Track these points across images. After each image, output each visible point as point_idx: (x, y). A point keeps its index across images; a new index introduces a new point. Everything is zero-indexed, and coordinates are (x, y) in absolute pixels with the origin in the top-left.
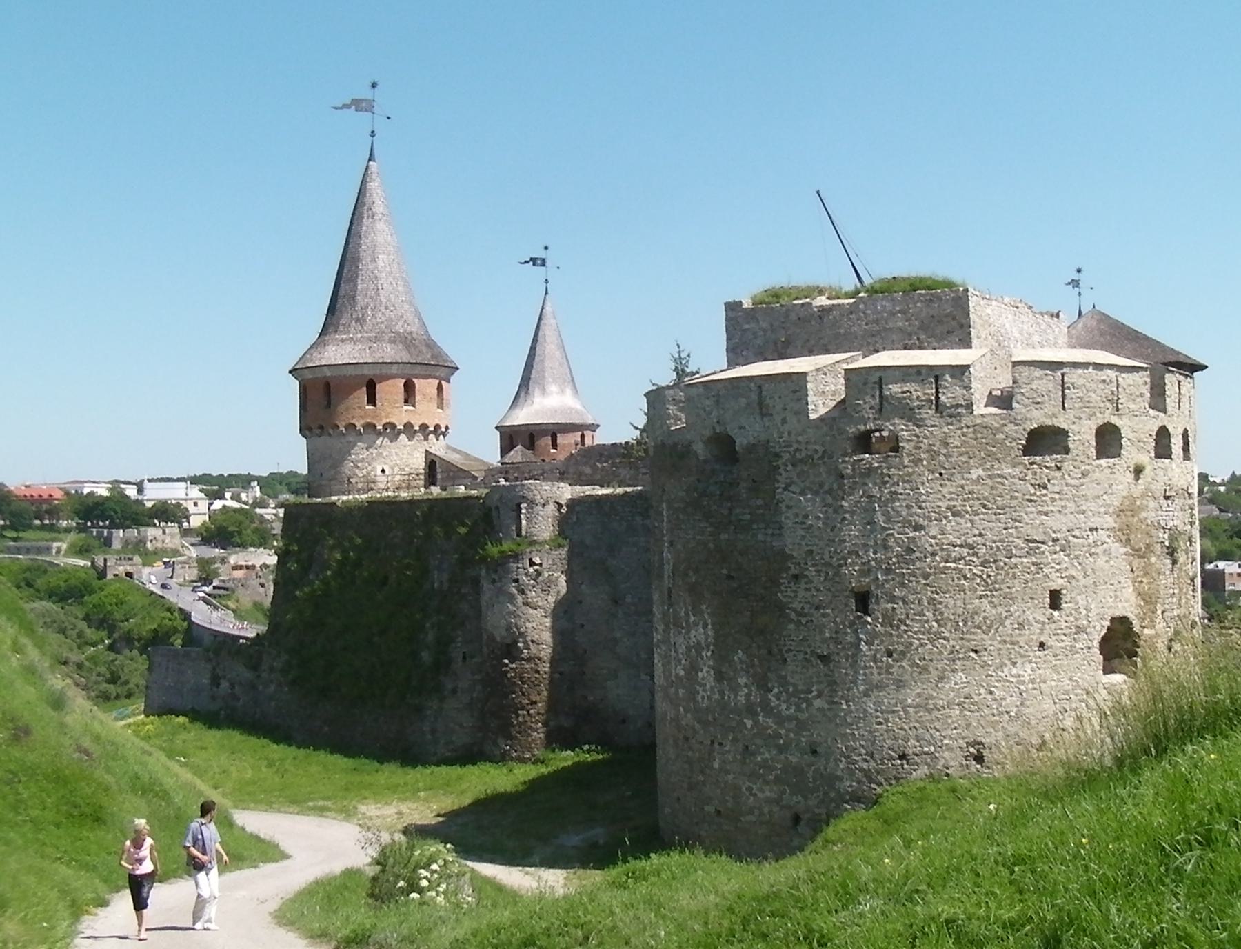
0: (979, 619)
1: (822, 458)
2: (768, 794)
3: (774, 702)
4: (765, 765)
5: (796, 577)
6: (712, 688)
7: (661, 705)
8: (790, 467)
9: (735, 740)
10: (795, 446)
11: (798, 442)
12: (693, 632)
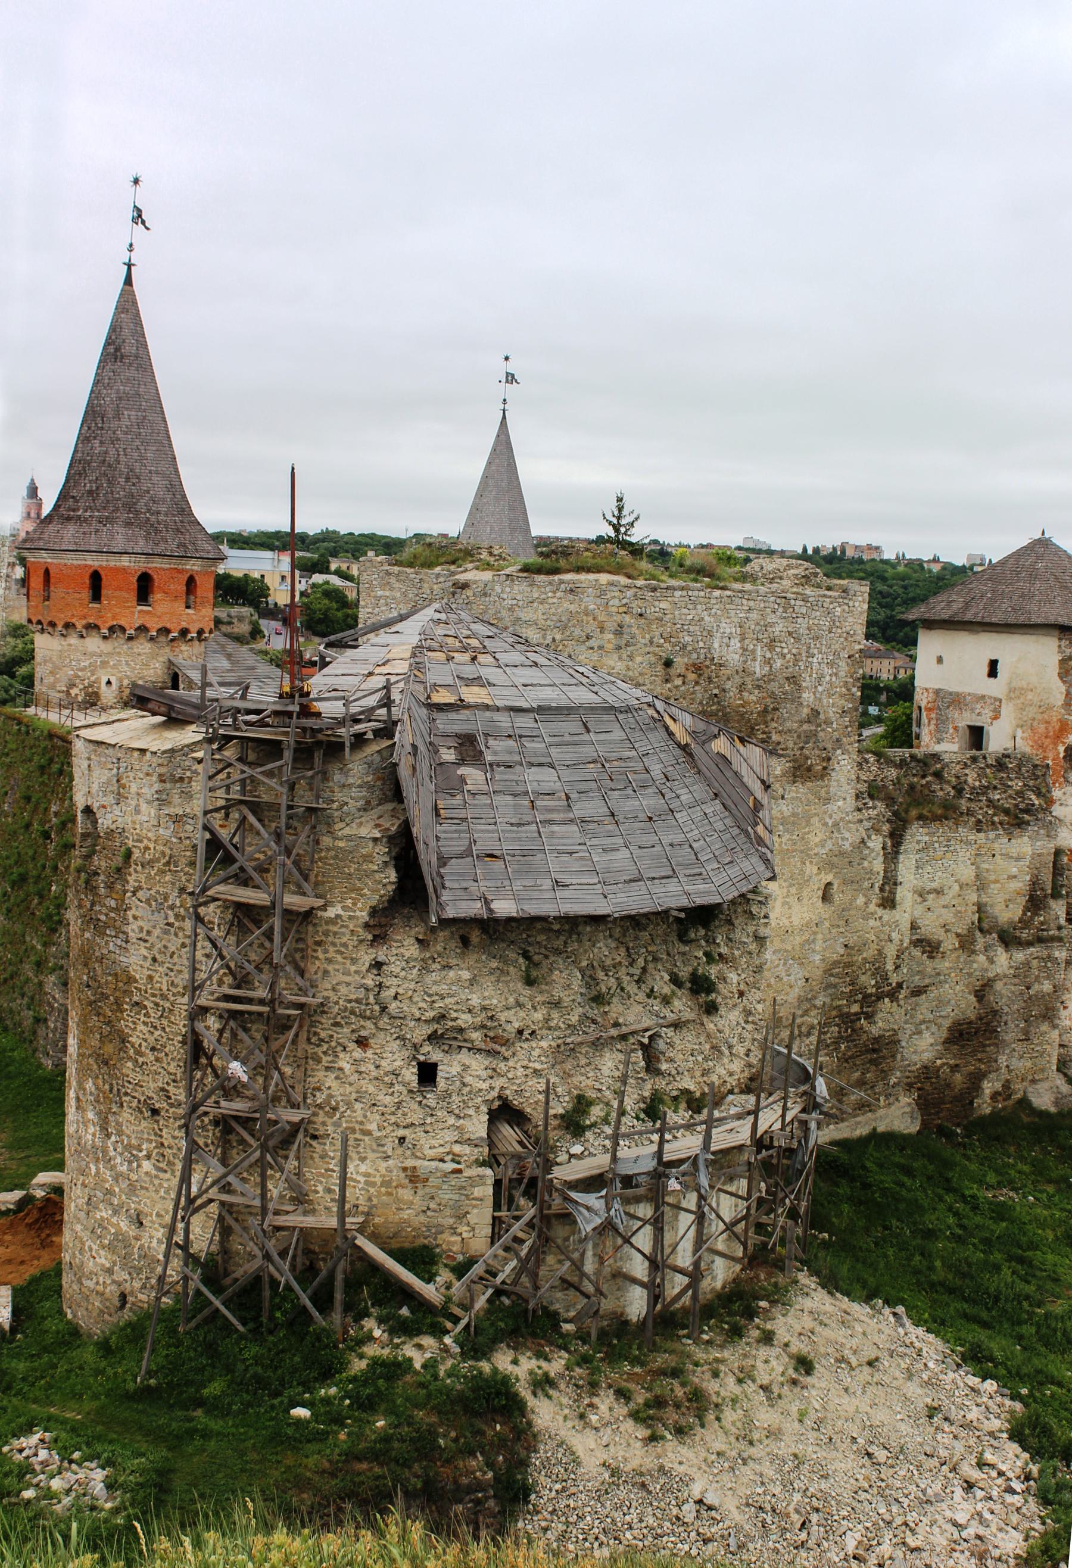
0: (320, 1098)
1: (168, 863)
2: (103, 1261)
8: (139, 868)
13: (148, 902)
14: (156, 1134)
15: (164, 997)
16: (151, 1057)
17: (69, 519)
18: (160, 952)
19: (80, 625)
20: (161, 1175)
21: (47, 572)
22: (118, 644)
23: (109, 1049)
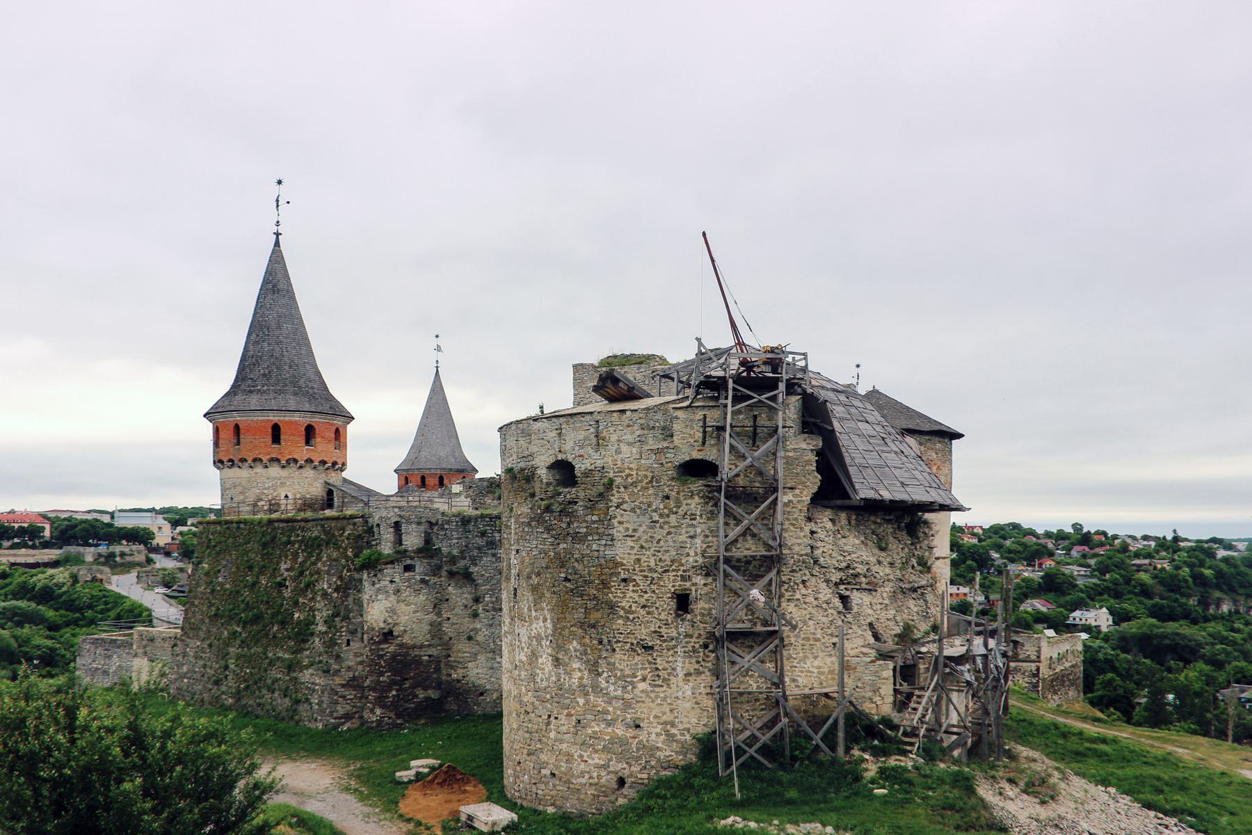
1: (651, 482)
2: (597, 761)
3: (604, 684)
4: (594, 736)
5: (624, 580)
6: (550, 672)
7: (507, 685)
8: (622, 489)
9: (569, 715)
10: (627, 471)
11: (631, 469)
12: (534, 625)
13: (633, 510)
14: (650, 663)
15: (651, 570)
16: (643, 612)
17: (251, 392)
18: (646, 541)
19: (265, 459)
20: (657, 689)
21: (237, 427)
22: (292, 471)
23: (595, 616)
